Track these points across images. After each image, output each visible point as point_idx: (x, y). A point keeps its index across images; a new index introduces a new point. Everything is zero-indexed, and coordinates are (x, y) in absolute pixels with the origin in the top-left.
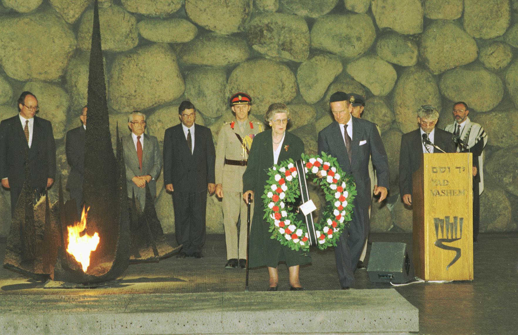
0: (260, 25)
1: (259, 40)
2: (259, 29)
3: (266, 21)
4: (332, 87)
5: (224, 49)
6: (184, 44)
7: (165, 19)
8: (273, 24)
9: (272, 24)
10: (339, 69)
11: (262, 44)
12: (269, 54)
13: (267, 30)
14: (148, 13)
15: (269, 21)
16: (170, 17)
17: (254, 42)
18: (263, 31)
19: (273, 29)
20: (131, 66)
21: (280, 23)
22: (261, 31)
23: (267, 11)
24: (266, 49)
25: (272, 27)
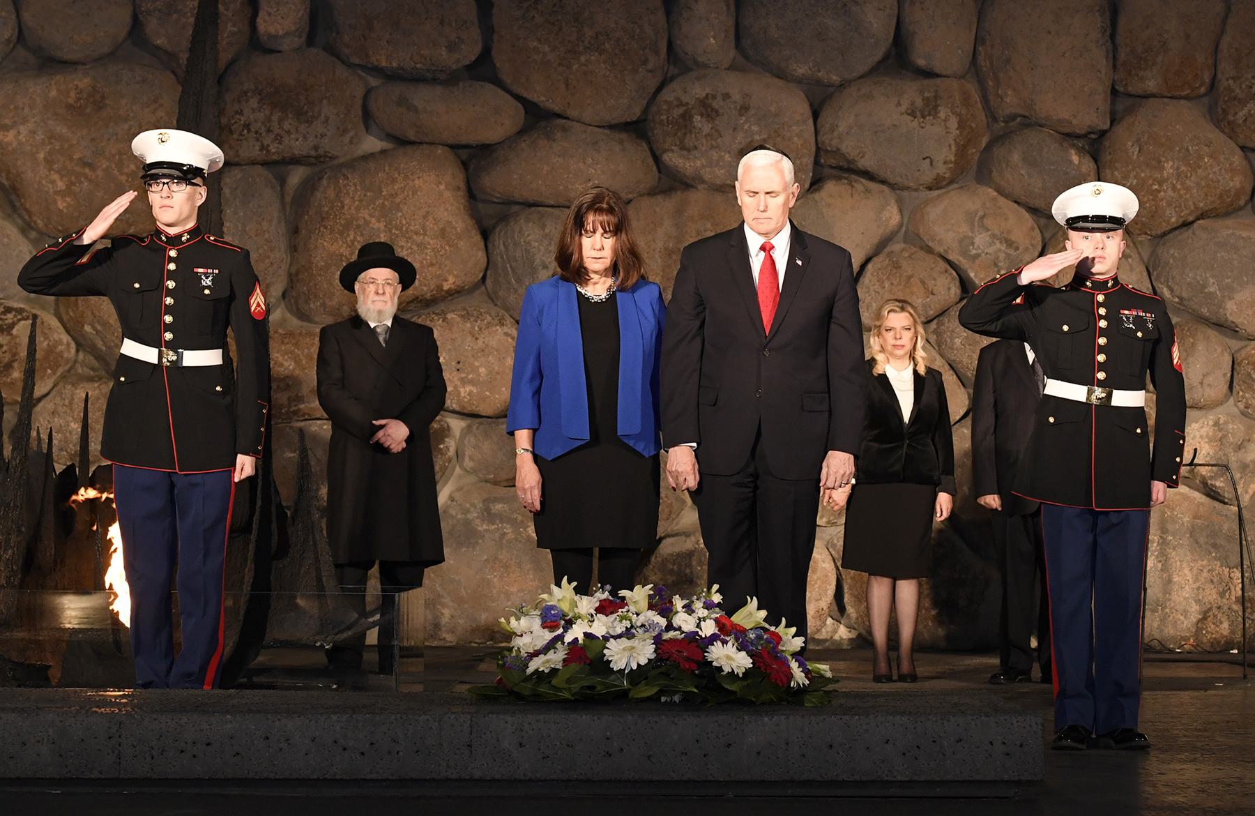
0: (685, 99)
1: (682, 142)
2: (681, 110)
3: (699, 91)
4: (870, 266)
5: (589, 161)
6: (486, 149)
7: (435, 81)
8: (719, 98)
9: (714, 97)
10: (892, 216)
11: (689, 150)
12: (707, 177)
13: (702, 115)
14: (394, 65)
15: (708, 91)
16: (449, 79)
17: (666, 146)
18: (691, 117)
19: (717, 112)
20: (347, 201)
21: (736, 97)
22: (687, 116)
23: (706, 66)
24: (698, 163)
25: (715, 105)
